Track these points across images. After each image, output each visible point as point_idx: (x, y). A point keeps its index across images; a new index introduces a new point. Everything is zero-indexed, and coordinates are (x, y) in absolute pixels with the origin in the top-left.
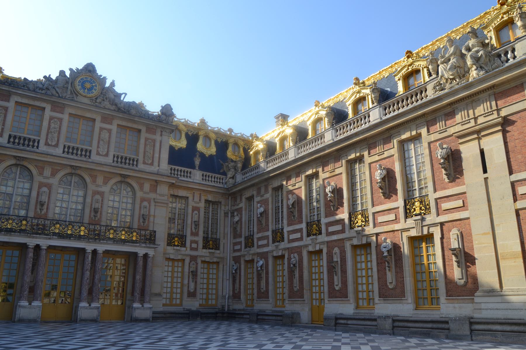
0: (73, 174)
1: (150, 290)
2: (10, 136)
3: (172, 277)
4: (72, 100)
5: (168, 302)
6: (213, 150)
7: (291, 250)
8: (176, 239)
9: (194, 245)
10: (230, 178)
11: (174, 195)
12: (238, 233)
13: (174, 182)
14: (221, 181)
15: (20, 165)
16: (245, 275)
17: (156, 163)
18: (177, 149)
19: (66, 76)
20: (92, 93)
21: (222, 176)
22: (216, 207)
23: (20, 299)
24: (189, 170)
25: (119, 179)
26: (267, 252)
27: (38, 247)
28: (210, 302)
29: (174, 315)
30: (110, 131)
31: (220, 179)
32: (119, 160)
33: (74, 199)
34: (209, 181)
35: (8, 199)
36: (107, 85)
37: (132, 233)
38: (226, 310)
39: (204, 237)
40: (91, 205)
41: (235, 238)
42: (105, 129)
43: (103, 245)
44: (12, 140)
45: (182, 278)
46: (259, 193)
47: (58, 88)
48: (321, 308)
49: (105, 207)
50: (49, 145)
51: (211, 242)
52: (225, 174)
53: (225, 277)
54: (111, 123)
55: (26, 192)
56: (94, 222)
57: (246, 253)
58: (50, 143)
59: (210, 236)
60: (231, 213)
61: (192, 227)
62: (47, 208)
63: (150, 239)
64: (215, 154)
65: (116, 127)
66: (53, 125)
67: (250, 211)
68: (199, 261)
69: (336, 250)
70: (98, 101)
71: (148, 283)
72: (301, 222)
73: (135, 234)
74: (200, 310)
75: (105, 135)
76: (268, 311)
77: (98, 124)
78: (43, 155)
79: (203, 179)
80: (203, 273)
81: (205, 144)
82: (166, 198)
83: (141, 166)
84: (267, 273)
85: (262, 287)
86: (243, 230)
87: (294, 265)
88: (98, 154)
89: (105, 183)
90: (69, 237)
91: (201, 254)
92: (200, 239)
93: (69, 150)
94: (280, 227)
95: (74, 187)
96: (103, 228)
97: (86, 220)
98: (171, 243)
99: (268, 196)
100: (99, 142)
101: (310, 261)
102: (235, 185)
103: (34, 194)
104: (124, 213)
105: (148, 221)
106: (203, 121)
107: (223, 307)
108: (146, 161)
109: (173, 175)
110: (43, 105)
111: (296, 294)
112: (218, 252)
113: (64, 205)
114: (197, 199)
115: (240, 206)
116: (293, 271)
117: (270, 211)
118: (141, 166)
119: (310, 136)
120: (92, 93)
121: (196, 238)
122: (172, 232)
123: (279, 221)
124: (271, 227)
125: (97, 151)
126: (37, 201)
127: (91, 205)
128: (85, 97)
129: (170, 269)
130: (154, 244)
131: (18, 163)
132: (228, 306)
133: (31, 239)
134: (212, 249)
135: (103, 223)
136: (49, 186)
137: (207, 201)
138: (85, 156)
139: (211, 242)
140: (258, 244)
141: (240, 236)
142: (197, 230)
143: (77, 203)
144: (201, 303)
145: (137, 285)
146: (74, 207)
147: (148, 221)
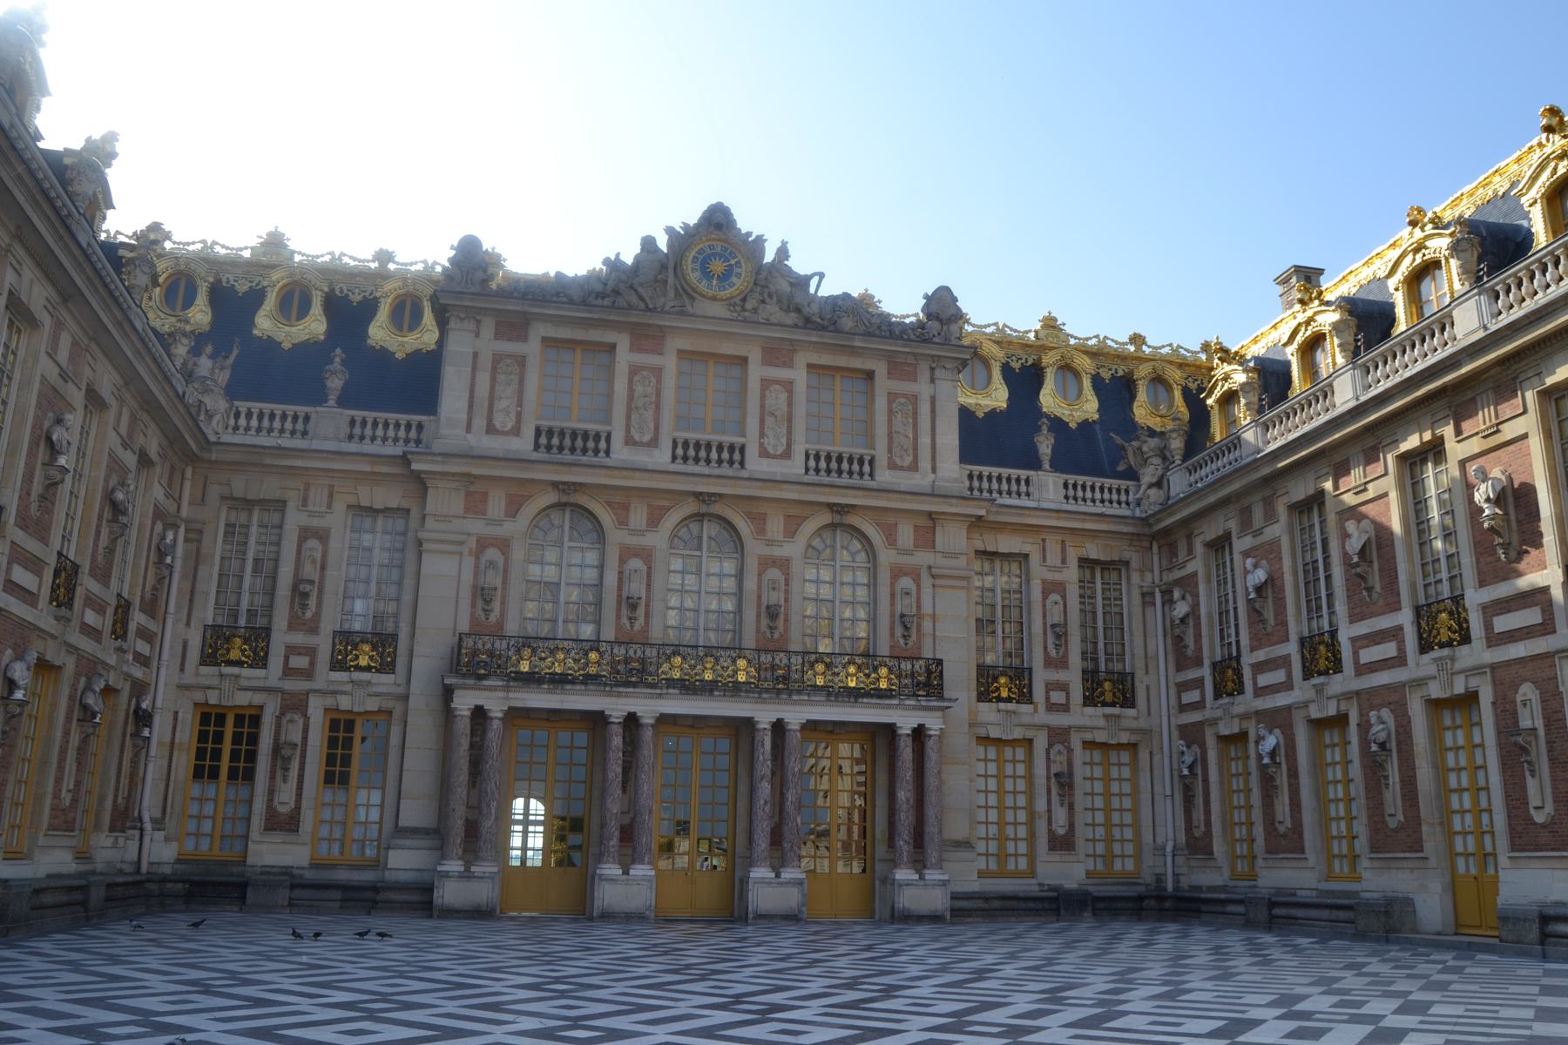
0: (703, 515)
1: (940, 831)
2: (538, 432)
3: (1001, 792)
4: (682, 313)
5: (993, 866)
6: (1090, 407)
7: (1368, 699)
8: (1002, 680)
9: (1058, 697)
10: (1151, 486)
11: (985, 553)
12: (1189, 652)
13: (982, 512)
14: (1123, 498)
15: (571, 504)
16: (1221, 782)
17: (925, 464)
18: (980, 415)
19: (657, 250)
20: (732, 285)
21: (1124, 484)
22: (1114, 575)
23: (600, 858)
24: (1023, 473)
25: (826, 518)
26: (1288, 709)
27: (631, 720)
28: (1118, 866)
29: (1014, 904)
30: (788, 386)
31: (1119, 491)
32: (823, 465)
33: (714, 583)
34: (1084, 500)
35: (549, 597)
36: (769, 257)
37: (875, 669)
38: (1170, 888)
39: (1084, 672)
40: (759, 597)
41: (1180, 668)
42: (777, 382)
43: (798, 708)
44: (543, 440)
45: (1030, 793)
46: (1246, 524)
47: (641, 285)
48: (1486, 886)
49: (795, 600)
50: (635, 444)
51: (1107, 685)
52: (1131, 475)
53: (1157, 789)
54: (789, 364)
55: (591, 575)
56: (772, 644)
57: (1219, 713)
58: (637, 437)
59: (1102, 667)
60: (1163, 593)
61: (1045, 642)
62: (647, 615)
63: (927, 685)
64: (1096, 417)
65: (804, 372)
66: (639, 389)
67: (1222, 582)
68: (1076, 741)
69: (1527, 691)
70: (749, 306)
71: (931, 812)
72: (1395, 607)
73: (883, 671)
74: (1091, 889)
75: (777, 399)
76: (1303, 893)
77: (757, 371)
78: (625, 473)
79: (1067, 497)
80: (1092, 779)
81: (1063, 392)
82: (962, 561)
83: (884, 476)
84: (1293, 774)
85: (1279, 817)
86: (1205, 641)
87: (1382, 746)
88: (764, 453)
89: (791, 533)
90: (708, 689)
91: (1082, 722)
92: (1073, 677)
93: (690, 451)
94: (1327, 628)
95: (709, 550)
96: (796, 661)
97: (749, 640)
98: (988, 692)
99: (1278, 530)
100: (762, 421)
101: (1436, 731)
102: (1167, 507)
103: (611, 579)
104: (848, 614)
105: (919, 631)
106: (1050, 324)
107: (1160, 879)
108: (898, 461)
109: (976, 493)
110: (609, 337)
111: (1396, 840)
112: (1131, 712)
113: (689, 603)
114: (1053, 557)
115: (1190, 568)
116: (1381, 766)
117: (1288, 579)
118: (884, 476)
119: (1401, 326)
120: (732, 285)
121: (1061, 676)
122: (989, 659)
123: (1319, 608)
124: (1296, 627)
125: (761, 445)
126: (619, 596)
127: (759, 597)
128: (714, 299)
129: (992, 769)
130: (941, 697)
131: (564, 499)
132: (1176, 875)
133: (614, 700)
134: (1113, 705)
135: (794, 647)
136: (646, 555)
137: (1085, 563)
138: (731, 462)
139: (1107, 685)
140: (1255, 683)
141: (1199, 662)
142: (1062, 651)
143: (720, 594)
144: (1091, 867)
145: (903, 816)
146: (714, 606)
147: (919, 631)
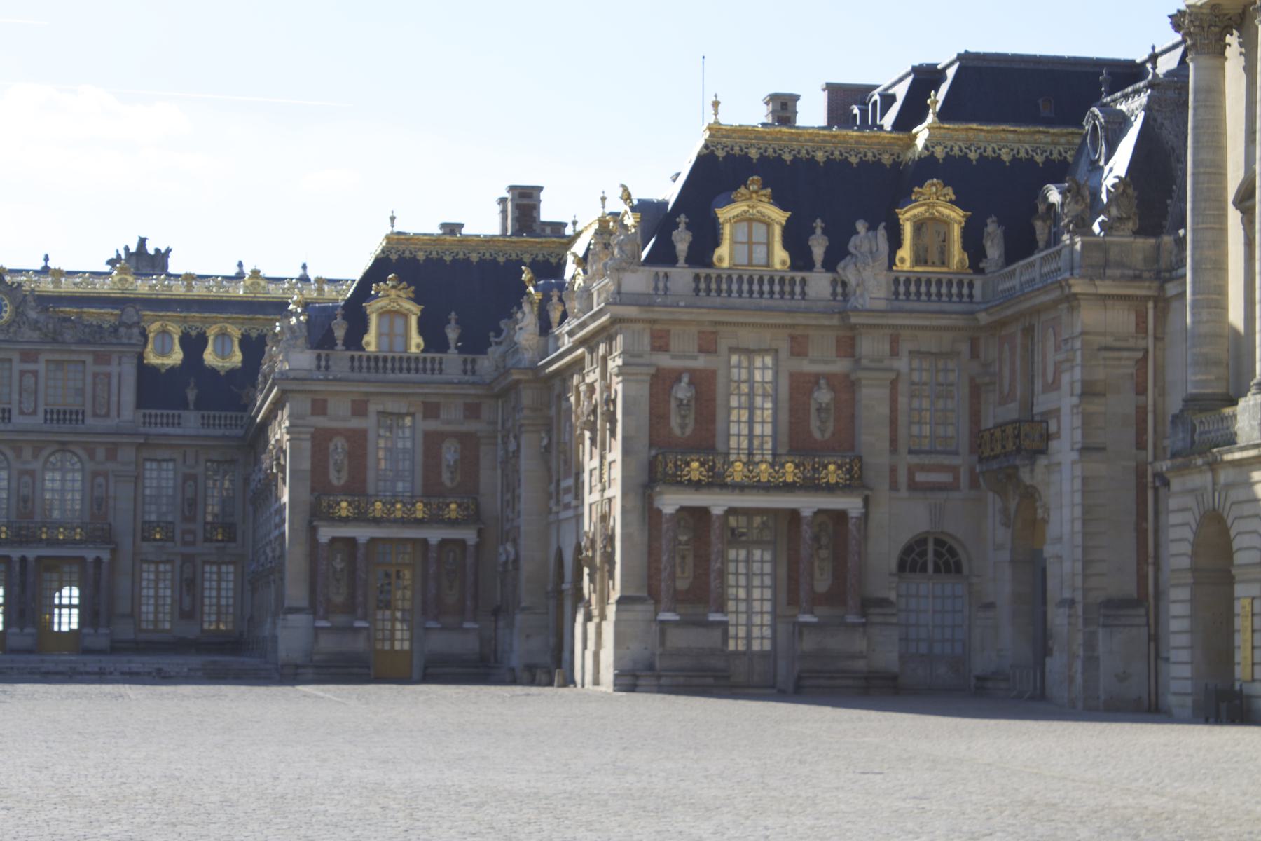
5: (151, 627)
9: (189, 538)
13: (142, 441)
17: (114, 413)
18: (163, 371)
21: (239, 414)
24: (176, 412)
30: (35, 374)
32: (55, 417)
54: (36, 361)
75: (29, 381)
77: (17, 366)
88: (22, 413)
89: (35, 456)
100: (20, 395)
112: (233, 545)
118: (90, 421)
